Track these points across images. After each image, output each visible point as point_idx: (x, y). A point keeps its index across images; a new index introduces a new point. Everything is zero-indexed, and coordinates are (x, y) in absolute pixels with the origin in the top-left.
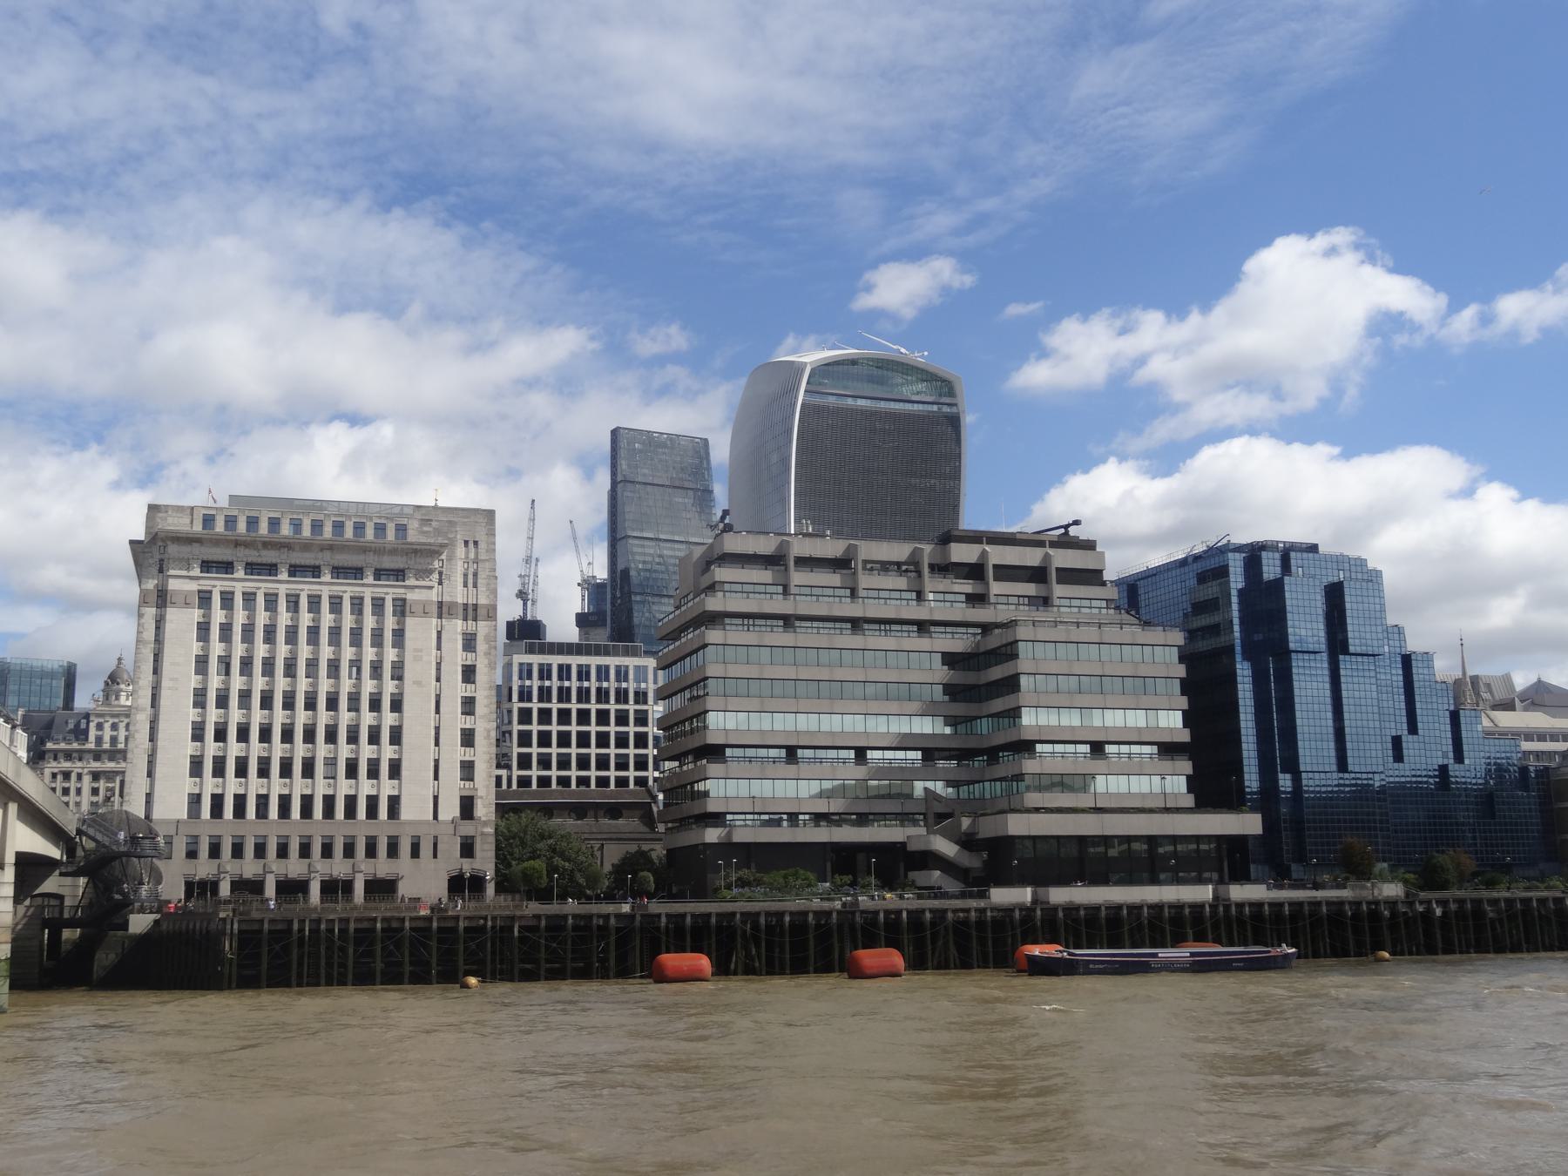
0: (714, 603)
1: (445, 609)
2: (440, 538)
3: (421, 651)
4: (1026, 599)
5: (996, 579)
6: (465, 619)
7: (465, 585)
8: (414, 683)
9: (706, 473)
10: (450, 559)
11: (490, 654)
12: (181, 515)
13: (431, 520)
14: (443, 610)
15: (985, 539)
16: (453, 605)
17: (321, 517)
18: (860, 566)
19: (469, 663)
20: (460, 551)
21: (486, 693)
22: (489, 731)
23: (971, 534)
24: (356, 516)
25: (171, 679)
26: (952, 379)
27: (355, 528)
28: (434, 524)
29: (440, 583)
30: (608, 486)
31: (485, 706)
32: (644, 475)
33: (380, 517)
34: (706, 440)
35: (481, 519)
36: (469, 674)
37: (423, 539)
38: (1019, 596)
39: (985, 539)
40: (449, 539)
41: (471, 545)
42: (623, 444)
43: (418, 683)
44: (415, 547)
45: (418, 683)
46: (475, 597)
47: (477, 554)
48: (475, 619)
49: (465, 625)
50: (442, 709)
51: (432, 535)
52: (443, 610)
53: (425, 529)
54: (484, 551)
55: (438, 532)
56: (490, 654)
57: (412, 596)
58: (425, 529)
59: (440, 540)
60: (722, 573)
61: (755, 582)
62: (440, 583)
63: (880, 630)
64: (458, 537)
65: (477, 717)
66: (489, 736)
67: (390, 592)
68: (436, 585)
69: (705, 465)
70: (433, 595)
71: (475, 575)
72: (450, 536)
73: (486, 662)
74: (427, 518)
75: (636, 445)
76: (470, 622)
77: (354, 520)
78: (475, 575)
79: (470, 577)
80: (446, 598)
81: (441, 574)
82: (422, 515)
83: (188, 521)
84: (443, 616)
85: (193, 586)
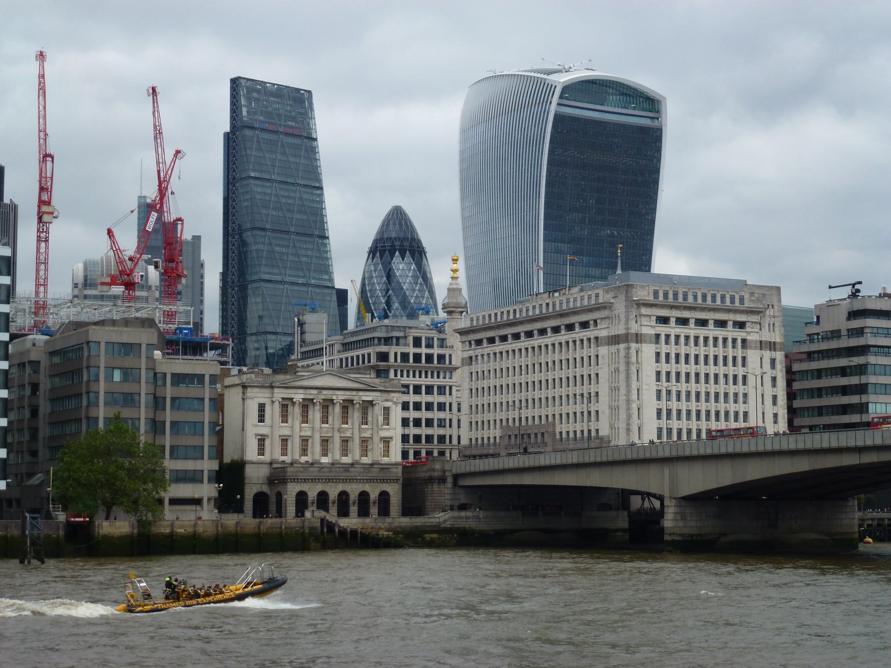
1: (763, 345)
10: (764, 316)
14: (762, 345)
19: (773, 376)
24: (721, 291)
25: (647, 384)
28: (756, 295)
29: (760, 330)
32: (260, 121)
33: (732, 292)
35: (775, 292)
41: (771, 307)
42: (243, 92)
47: (774, 312)
50: (765, 402)
52: (762, 345)
53: (752, 298)
57: (749, 338)
58: (752, 298)
62: (760, 329)
67: (740, 334)
68: (758, 330)
71: (774, 324)
73: (781, 375)
76: (773, 352)
78: (774, 324)
79: (772, 326)
80: (764, 339)
81: (760, 324)
83: (646, 293)
84: (763, 349)
85: (652, 332)
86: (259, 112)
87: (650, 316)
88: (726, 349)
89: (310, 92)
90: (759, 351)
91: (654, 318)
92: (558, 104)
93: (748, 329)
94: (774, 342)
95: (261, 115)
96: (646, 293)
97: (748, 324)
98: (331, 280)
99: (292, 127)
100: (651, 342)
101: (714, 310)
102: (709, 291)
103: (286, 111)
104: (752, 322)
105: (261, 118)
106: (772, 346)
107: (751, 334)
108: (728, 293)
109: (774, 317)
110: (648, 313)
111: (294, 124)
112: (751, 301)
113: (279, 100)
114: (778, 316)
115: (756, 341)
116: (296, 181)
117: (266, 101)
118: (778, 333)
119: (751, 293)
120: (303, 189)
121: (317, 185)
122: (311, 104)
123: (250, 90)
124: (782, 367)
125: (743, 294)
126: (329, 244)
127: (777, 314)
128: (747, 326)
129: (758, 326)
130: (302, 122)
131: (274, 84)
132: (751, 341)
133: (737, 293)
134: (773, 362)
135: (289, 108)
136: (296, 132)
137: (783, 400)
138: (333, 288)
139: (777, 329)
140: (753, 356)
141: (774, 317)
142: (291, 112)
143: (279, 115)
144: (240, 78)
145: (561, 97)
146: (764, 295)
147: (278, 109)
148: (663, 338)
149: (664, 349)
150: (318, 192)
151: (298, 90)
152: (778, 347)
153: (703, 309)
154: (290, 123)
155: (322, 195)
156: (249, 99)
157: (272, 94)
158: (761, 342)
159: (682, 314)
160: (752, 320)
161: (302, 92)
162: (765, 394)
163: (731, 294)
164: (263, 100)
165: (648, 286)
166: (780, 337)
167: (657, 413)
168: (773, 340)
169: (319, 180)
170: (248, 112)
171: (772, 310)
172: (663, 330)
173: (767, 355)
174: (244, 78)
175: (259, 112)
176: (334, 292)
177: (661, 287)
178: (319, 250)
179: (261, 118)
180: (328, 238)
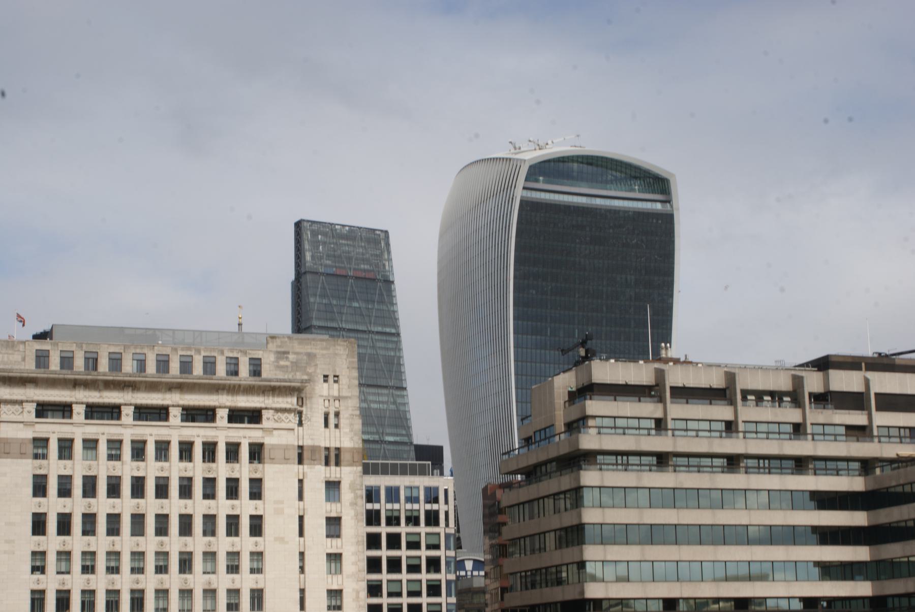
0: (589, 441)
1: (306, 455)
2: (298, 374)
3: (282, 502)
4: (907, 431)
5: (879, 408)
6: (327, 463)
7: (326, 425)
8: (276, 539)
9: (387, 264)
11: (356, 504)
12: (10, 352)
13: (288, 353)
15: (863, 365)
16: (314, 449)
17: (167, 351)
18: (739, 397)
20: (323, 389)
21: (353, 549)
22: (358, 592)
23: (850, 360)
24: (206, 350)
26: (664, 175)
27: (205, 363)
28: (291, 357)
29: (300, 424)
30: (292, 276)
31: (353, 564)
32: (326, 266)
33: (232, 351)
34: (386, 232)
36: (334, 525)
37: (281, 376)
38: (900, 428)
39: (863, 365)
40: (308, 374)
41: (331, 379)
42: (307, 235)
43: (281, 540)
44: (273, 384)
45: (281, 540)
46: (338, 439)
48: (338, 464)
49: (328, 471)
51: (290, 369)
53: (282, 363)
54: (346, 387)
55: (296, 365)
56: (356, 504)
57: (268, 441)
58: (282, 363)
59: (299, 376)
60: (594, 406)
61: (629, 415)
62: (300, 424)
63: (759, 468)
64: (318, 371)
65: (344, 576)
66: (358, 597)
67: (245, 435)
68: (296, 427)
69: (386, 256)
70: (291, 440)
72: (310, 370)
73: (352, 513)
74: (282, 350)
75: (320, 237)
76: (333, 468)
77: (203, 354)
78: (337, 415)
80: (307, 442)
81: (300, 413)
82: (277, 346)
84: (305, 461)
85: (28, 434)
86: (325, 256)
87: (20, 403)
88: (213, 465)
89: (386, 232)
90: (296, 467)
91: (32, 407)
92: (524, 188)
93: (265, 424)
94: (338, 449)
95: (326, 260)
96: (17, 357)
97: (265, 414)
98: (409, 435)
99: (365, 271)
100: (22, 455)
101: (181, 387)
102: (125, 347)
103: (357, 254)
104: (277, 410)
105: (329, 262)
106: (333, 457)
107: (275, 432)
108: (222, 353)
109: (338, 399)
110: (15, 397)
111: (367, 267)
112: (279, 367)
113: (351, 243)
114: (346, 398)
115: (286, 448)
116: (367, 327)
117: (333, 243)
118: (347, 430)
119: (278, 352)
120: (377, 337)
121: (393, 331)
122: (388, 245)
123: (315, 234)
124: (356, 497)
125: (258, 354)
126: (407, 396)
127: (345, 393)
128: (264, 417)
129: (293, 419)
130: (377, 266)
131: (344, 226)
132: (274, 447)
133: (245, 353)
134: (333, 486)
135: (347, 249)
136: (371, 275)
137: (355, 563)
138: (411, 443)
139: (343, 422)
140: (272, 473)
141: (338, 399)
142: (363, 254)
143: (349, 259)
144: (304, 220)
145: (527, 180)
146: (311, 356)
147: (349, 252)
148: (53, 446)
149: (54, 467)
150: (395, 339)
151: (373, 230)
152: (345, 457)
153: (153, 387)
154: (362, 266)
155: (398, 343)
156: (315, 244)
157: (342, 236)
158: (301, 448)
159: (101, 397)
160: (274, 406)
161: (378, 232)
162: (306, 554)
163: (231, 355)
164: (330, 243)
165: (270, 371)
166: (352, 439)
167: (33, 601)
168: (333, 444)
169: (396, 326)
170: (313, 257)
171: (336, 385)
172: (53, 429)
173: (316, 474)
174: (308, 221)
175: (325, 256)
176: (413, 448)
177: (80, 346)
178: (394, 403)
179: (329, 262)
180: (405, 389)
